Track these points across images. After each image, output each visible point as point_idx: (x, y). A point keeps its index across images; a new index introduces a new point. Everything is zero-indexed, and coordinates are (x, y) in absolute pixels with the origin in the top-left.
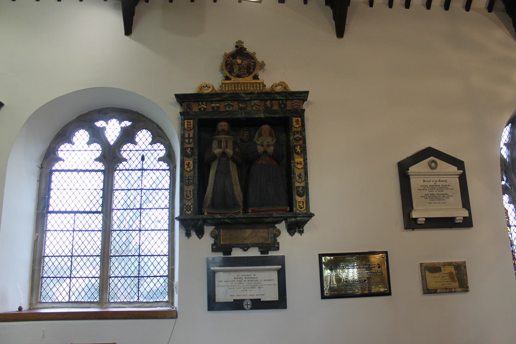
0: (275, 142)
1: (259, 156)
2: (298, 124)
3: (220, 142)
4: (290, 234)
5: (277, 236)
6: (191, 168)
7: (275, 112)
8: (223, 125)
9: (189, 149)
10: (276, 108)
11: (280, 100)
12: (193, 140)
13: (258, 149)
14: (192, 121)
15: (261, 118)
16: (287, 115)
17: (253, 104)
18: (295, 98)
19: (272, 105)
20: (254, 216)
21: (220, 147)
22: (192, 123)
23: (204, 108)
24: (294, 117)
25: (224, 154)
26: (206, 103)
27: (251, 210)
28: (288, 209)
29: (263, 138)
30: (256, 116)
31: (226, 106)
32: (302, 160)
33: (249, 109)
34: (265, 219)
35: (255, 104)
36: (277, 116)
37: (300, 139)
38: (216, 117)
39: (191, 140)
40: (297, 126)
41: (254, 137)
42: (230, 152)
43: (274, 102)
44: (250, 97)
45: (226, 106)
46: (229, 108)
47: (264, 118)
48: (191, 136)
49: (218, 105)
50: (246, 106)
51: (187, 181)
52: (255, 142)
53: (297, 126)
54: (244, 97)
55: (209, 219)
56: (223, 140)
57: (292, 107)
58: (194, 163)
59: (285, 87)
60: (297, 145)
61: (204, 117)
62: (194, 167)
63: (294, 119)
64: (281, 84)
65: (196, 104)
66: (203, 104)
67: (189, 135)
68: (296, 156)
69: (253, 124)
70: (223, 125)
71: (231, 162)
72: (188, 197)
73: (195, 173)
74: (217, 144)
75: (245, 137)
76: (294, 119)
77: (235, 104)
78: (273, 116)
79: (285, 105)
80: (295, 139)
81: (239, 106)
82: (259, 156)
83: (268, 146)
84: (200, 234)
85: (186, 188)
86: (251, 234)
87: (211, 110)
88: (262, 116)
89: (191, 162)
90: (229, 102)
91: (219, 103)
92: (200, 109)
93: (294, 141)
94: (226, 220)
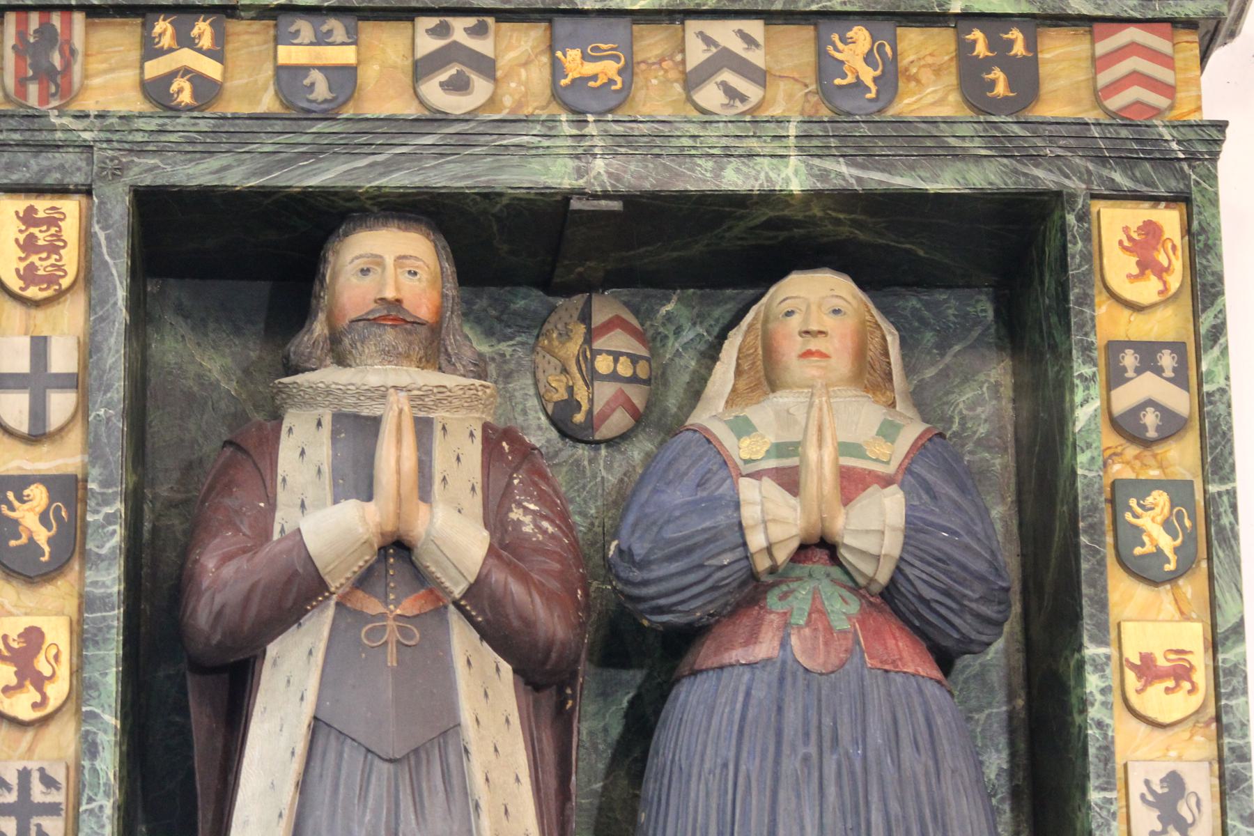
0: (919, 449)
1: (751, 590)
2: (1147, 266)
3: (357, 431)
6: (57, 691)
7: (923, 141)
8: (386, 266)
9: (38, 494)
10: (931, 96)
12: (83, 408)
13: (750, 514)
14: (71, 207)
15: (768, 198)
16: (1046, 178)
17: (697, 54)
19: (891, 77)
21: (357, 479)
22: (70, 229)
23: (200, 82)
24: (1118, 196)
25: (397, 549)
26: (220, 37)
29: (783, 399)
30: (734, 179)
31: (421, 69)
32: (1193, 636)
33: (656, 100)
36: (944, 181)
37: (1172, 426)
38: (326, 175)
39: (61, 405)
40: (1147, 291)
41: (695, 392)
42: (457, 538)
43: (916, 44)
45: (421, 69)
46: (458, 85)
47: (814, 196)
48: (63, 359)
49: (347, 55)
50: (628, 71)
52: (709, 440)
53: (1147, 291)
56: (395, 415)
57: (1099, 96)
58: (82, 638)
60: (1143, 487)
62: (81, 687)
63: (1116, 222)
65: (119, 40)
66: (185, 40)
67: (40, 347)
68: (1125, 597)
69: (710, 252)
71: (463, 640)
73: (90, 748)
74: (322, 451)
75: (605, 392)
76: (1116, 222)
77: (518, 47)
78: (903, 181)
79: (1027, 79)
80: (1126, 427)
81: (556, 69)
82: (751, 590)
83: (852, 483)
87: (267, 103)
88: (792, 177)
89: (58, 634)
90: (459, 26)
91: (353, 39)
92: (156, 91)
93: (1110, 440)
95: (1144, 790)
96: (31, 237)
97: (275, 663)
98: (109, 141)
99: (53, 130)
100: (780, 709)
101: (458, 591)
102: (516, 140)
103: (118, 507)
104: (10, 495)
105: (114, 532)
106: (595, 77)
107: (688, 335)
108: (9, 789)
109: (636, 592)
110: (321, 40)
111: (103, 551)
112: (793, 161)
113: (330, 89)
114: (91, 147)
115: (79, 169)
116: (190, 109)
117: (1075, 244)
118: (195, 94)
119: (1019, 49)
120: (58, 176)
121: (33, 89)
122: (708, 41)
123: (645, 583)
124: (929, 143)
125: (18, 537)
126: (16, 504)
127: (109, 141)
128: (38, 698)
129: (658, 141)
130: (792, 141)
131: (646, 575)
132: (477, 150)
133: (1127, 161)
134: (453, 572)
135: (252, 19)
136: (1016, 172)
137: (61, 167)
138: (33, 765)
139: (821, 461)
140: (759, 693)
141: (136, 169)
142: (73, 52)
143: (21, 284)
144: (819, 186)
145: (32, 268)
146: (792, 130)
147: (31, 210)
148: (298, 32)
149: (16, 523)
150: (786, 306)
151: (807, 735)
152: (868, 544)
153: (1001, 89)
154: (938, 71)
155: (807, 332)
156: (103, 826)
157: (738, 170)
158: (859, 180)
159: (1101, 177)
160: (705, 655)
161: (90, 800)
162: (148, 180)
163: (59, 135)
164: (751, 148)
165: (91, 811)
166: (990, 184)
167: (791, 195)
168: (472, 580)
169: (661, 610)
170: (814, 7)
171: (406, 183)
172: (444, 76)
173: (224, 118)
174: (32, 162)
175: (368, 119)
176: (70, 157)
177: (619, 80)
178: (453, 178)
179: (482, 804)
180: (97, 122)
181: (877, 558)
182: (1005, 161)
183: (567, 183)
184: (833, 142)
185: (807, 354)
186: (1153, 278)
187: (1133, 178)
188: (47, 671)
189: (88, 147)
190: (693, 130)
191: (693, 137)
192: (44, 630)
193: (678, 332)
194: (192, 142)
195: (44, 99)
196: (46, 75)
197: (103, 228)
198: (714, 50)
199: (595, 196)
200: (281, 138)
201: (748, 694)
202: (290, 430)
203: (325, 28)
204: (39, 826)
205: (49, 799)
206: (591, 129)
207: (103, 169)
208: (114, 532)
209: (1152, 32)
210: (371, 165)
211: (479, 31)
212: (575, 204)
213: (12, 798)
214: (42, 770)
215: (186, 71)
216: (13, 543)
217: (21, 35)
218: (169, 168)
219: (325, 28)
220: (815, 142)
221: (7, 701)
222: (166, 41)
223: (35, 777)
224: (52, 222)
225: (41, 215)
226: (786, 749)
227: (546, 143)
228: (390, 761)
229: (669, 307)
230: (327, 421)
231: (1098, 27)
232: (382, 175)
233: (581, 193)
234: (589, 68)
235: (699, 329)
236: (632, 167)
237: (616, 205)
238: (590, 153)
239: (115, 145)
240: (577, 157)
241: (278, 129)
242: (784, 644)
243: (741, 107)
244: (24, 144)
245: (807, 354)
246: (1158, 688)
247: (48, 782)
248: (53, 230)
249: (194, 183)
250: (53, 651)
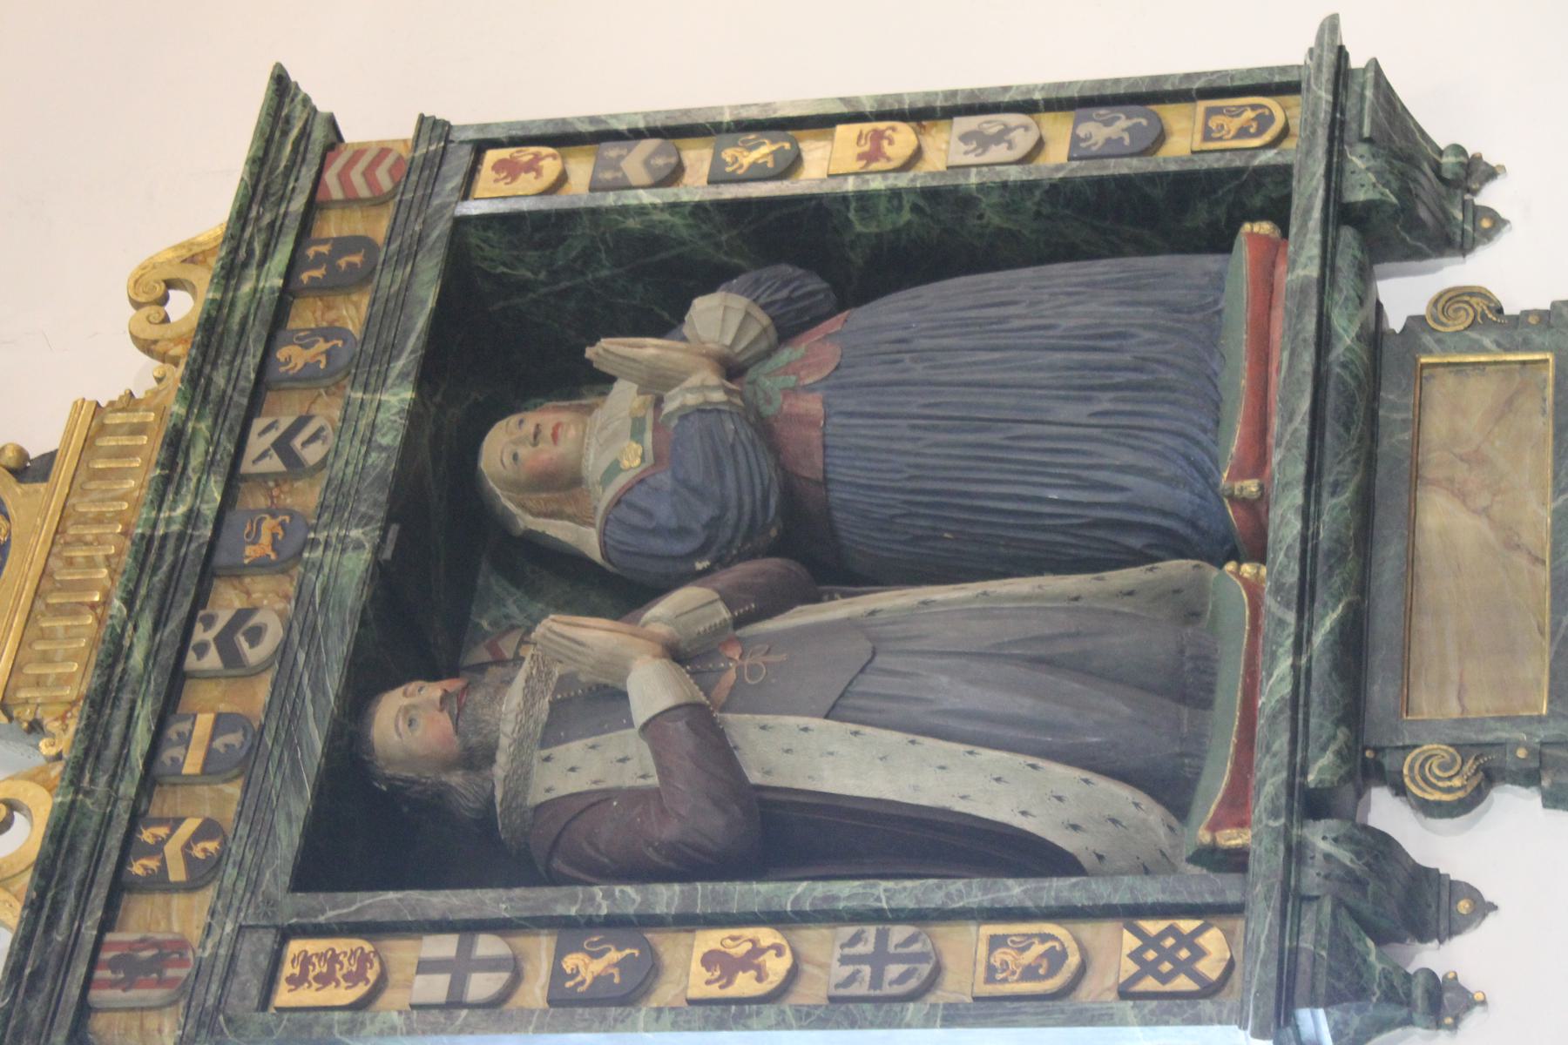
4: (1488, 236)
5: (1500, 311)
9: (570, 962)
11: (290, 273)
15: (414, 416)
17: (274, 464)
18: (307, 175)
20: (1305, 405)
22: (314, 946)
23: (198, 836)
26: (160, 822)
27: (1239, 473)
28: (1264, 227)
34: (1338, 352)
35: (283, 447)
36: (428, 295)
38: (316, 737)
39: (488, 946)
44: (209, 466)
46: (255, 635)
47: (419, 386)
48: (444, 946)
49: (205, 722)
51: (894, 970)
54: (192, 517)
55: (1296, 770)
59: (191, 260)
61: (288, 838)
64: (152, 293)
66: (157, 848)
70: (408, 723)
72: (1056, 959)
78: (421, 322)
81: (261, 566)
84: (1430, 904)
85: (959, 984)
86: (1462, 496)
88: (398, 397)
90: (199, 634)
92: (201, 874)
94: (1318, 639)
96: (317, 978)
97: (768, 773)
98: (239, 910)
99: (215, 956)
100: (869, 385)
101: (724, 614)
102: (317, 592)
103: (598, 891)
104: (569, 984)
105: (622, 892)
106: (274, 536)
107: (512, 609)
108: (858, 971)
109: (746, 518)
110: (185, 740)
111: (638, 899)
112: (384, 397)
113: (234, 731)
114: (241, 927)
115: (260, 939)
116: (224, 843)
118: (210, 838)
119: (324, 249)
120: (262, 957)
121: (170, 973)
122: (264, 455)
123: (740, 506)
124: (391, 305)
125: (612, 975)
126: (579, 979)
127: (239, 910)
128: (773, 952)
129: (345, 489)
130: (368, 397)
131: (733, 503)
132: (320, 622)
134: (708, 610)
135: (150, 802)
136: (431, 249)
137: (254, 954)
138: (838, 953)
139: (656, 346)
140: (850, 405)
141: (272, 889)
142: (142, 941)
143: (361, 984)
144: (412, 378)
145: (347, 977)
146: (359, 395)
147: (290, 980)
148: (174, 760)
149: (597, 979)
150: (508, 460)
151: (896, 362)
152: (734, 321)
153: (356, 259)
154: (329, 308)
155: (535, 436)
156: (905, 889)
157: (384, 435)
158: (412, 352)
160: (811, 467)
161: (878, 899)
162: (286, 880)
163: (222, 951)
165: (888, 899)
167: (415, 402)
168: (716, 596)
169: (766, 499)
170: (253, 376)
171: (337, 676)
172: (245, 645)
173: (240, 814)
174: (243, 978)
175: (270, 702)
176: (246, 947)
177: (280, 518)
178: (341, 639)
179: (922, 598)
180: (217, 917)
181: (747, 314)
183: (366, 555)
184: (376, 368)
185: (555, 436)
186: (542, 163)
188: (748, 946)
189: (241, 930)
190: (341, 462)
191: (347, 463)
192: (706, 950)
193: (507, 617)
194: (257, 842)
195: (183, 962)
196: (159, 963)
197: (323, 912)
198: (272, 452)
199: (383, 539)
200: (271, 771)
201: (851, 415)
202: (548, 790)
203: (174, 737)
204: (896, 946)
205: (872, 940)
206: (322, 536)
207: (266, 914)
208: (622, 892)
209: (331, 164)
210: (314, 702)
211: (209, 622)
212: (387, 554)
213: (866, 970)
214: (842, 946)
215: (187, 847)
216: (617, 980)
217: (113, 984)
218: (278, 862)
219: (174, 737)
220: (373, 381)
221: (771, 978)
222: (153, 864)
223: (847, 951)
224: (306, 961)
225: (297, 971)
226: (905, 376)
227: (326, 570)
228: (874, 654)
229: (485, 624)
230: (545, 753)
231: (320, 196)
232: (325, 694)
233: (377, 550)
234: (265, 538)
235: (510, 602)
237: (394, 529)
238: (342, 540)
239: (244, 905)
240: (344, 550)
241: (262, 772)
242: (810, 389)
243: (329, 431)
244: (224, 983)
245: (555, 436)
246: (887, 149)
247: (855, 940)
248: (314, 960)
249: (297, 841)
250: (729, 942)
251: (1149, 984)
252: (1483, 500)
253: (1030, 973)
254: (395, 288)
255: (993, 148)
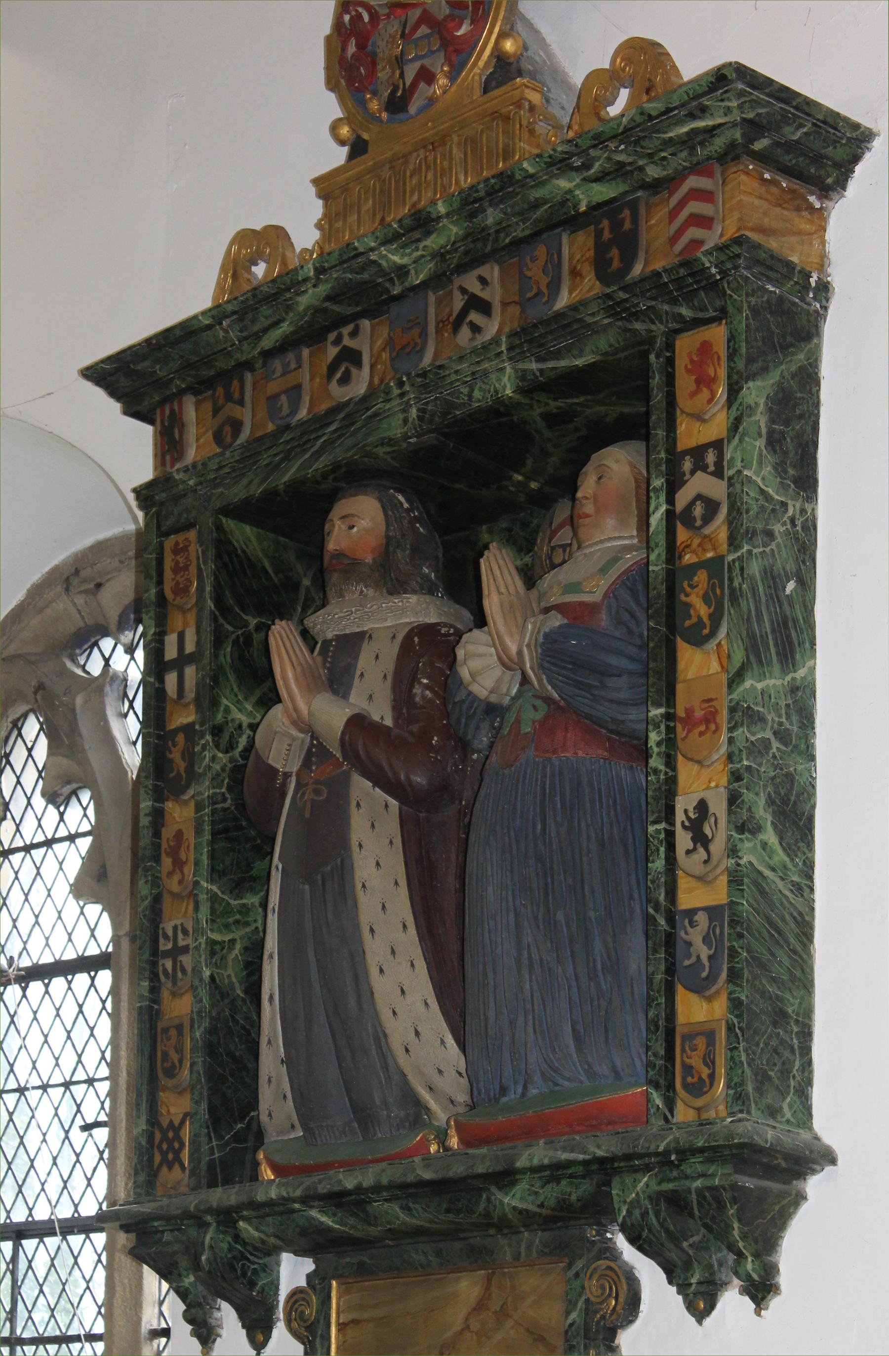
30: (480, 397)
95: (684, 818)
112: (508, 370)
117: (654, 378)
133: (689, 297)
146: (503, 348)
159: (673, 314)
164: (485, 369)
166: (611, 346)
182: (620, 323)
186: (705, 389)
187: (694, 308)
191: (457, 372)
206: (407, 388)
220: (518, 351)
236: (430, 408)
251: (158, 1136)
252: (475, 1326)
253: (165, 1055)
254: (590, 320)
255: (690, 835)
